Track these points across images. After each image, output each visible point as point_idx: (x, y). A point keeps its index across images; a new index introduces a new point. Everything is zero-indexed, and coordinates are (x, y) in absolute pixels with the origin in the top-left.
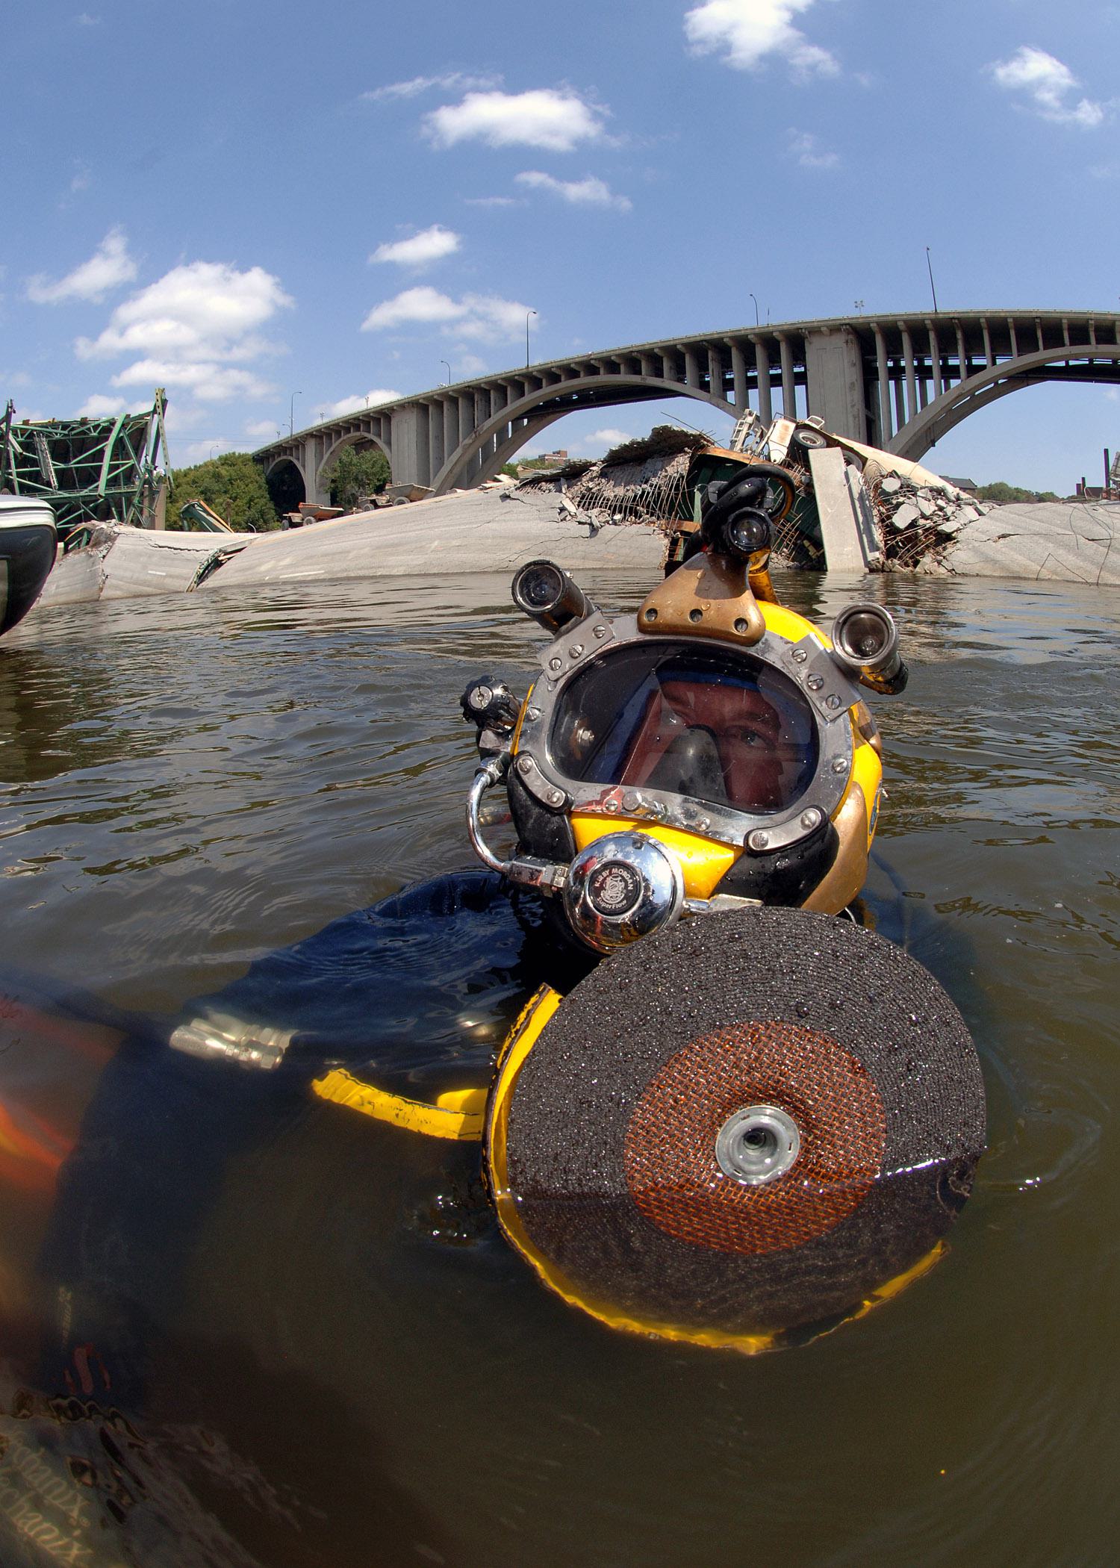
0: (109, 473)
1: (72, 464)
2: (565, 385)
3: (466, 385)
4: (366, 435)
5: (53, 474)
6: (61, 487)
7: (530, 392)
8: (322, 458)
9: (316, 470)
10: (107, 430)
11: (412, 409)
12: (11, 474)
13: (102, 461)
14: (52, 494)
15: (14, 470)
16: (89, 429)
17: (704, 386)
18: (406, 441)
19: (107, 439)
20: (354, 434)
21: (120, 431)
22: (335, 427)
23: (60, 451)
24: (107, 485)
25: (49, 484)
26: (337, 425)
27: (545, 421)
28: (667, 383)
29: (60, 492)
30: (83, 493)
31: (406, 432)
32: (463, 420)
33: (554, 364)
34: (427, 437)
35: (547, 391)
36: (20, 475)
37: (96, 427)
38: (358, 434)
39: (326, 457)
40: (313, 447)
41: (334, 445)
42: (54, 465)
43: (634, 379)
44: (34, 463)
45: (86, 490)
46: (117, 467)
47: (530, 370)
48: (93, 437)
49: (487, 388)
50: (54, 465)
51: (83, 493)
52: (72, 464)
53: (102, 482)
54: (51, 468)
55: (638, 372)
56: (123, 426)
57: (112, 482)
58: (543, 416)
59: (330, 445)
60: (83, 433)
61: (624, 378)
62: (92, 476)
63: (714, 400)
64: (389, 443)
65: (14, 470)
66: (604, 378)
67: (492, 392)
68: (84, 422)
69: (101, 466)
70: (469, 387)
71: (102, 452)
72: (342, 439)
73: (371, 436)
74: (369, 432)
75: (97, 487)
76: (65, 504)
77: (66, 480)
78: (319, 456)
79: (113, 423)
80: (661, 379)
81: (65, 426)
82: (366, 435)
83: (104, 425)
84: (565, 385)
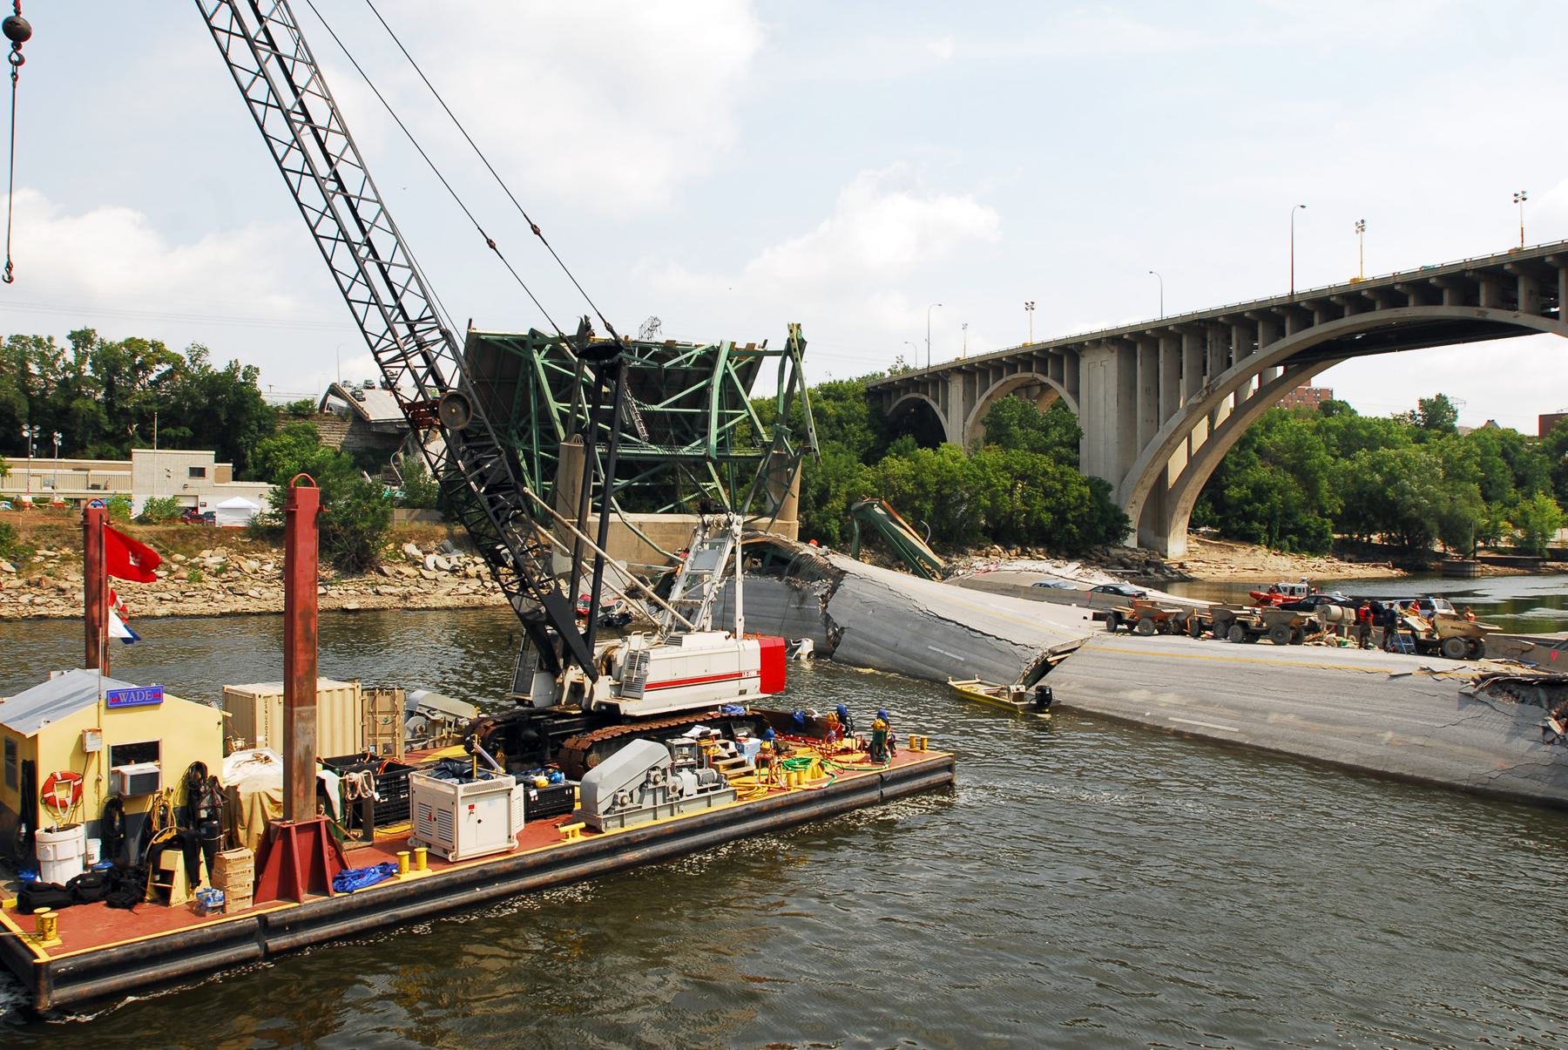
2: (1349, 321)
3: (1196, 317)
4: (1042, 378)
8: (973, 403)
9: (965, 420)
11: (1112, 348)
20: (1021, 375)
22: (995, 364)
26: (999, 360)
27: (1311, 370)
28: (1523, 319)
31: (1101, 375)
32: (1188, 368)
33: (1334, 292)
34: (1133, 387)
35: (1321, 330)
38: (1029, 375)
39: (979, 403)
40: (961, 387)
41: (992, 388)
47: (1296, 299)
58: (1313, 363)
61: (1447, 310)
64: (1075, 393)
66: (1414, 311)
67: (1234, 329)
70: (1200, 320)
72: (1003, 380)
73: (1048, 380)
74: (1046, 374)
78: (970, 400)
82: (1042, 378)
84: (1349, 321)
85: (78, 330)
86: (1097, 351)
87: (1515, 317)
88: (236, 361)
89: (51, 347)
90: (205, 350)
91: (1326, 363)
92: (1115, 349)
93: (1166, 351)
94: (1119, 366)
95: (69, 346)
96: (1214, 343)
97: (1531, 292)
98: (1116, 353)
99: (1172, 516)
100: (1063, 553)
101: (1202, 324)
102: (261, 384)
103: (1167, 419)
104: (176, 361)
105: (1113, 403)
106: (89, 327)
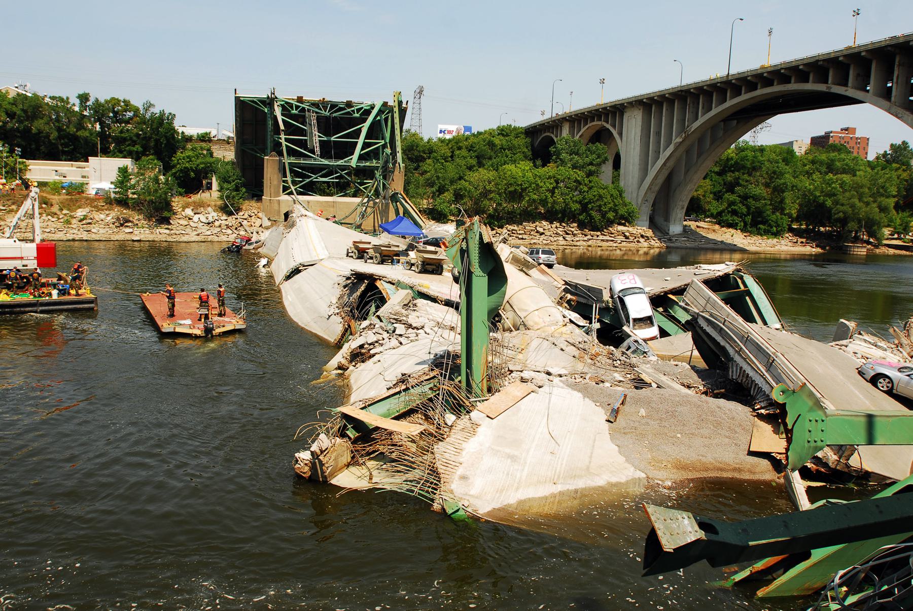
0: (362, 150)
1: (333, 139)
5: (318, 145)
6: (322, 156)
7: (732, 98)
10: (367, 112)
11: (640, 107)
12: (281, 139)
13: (358, 139)
14: (315, 159)
15: (283, 136)
16: (353, 111)
17: (886, 94)
18: (633, 132)
19: (364, 121)
21: (376, 116)
23: (326, 125)
24: (358, 160)
25: (313, 152)
28: (850, 92)
29: (322, 160)
30: (341, 162)
31: (633, 123)
32: (677, 120)
36: (286, 140)
37: (358, 110)
42: (319, 137)
43: (821, 87)
44: (302, 132)
45: (342, 161)
46: (369, 145)
48: (356, 118)
49: (711, 90)
50: (319, 137)
51: (341, 162)
52: (333, 139)
53: (355, 156)
54: (316, 138)
55: (826, 82)
56: (380, 112)
57: (361, 158)
59: (579, 130)
60: (348, 113)
61: (811, 86)
62: (346, 150)
63: (894, 109)
65: (283, 136)
68: (349, 104)
69: (365, 139)
71: (360, 130)
75: (351, 159)
76: (324, 169)
77: (327, 150)
79: (372, 107)
80: (844, 88)
81: (334, 106)
83: (366, 108)
85: (81, 93)
86: (632, 109)
87: (846, 91)
88: (163, 110)
89: (68, 103)
90: (154, 106)
91: (756, 120)
92: (641, 108)
93: (667, 110)
94: (642, 119)
95: (77, 102)
96: (691, 105)
97: (858, 75)
98: (641, 110)
99: (673, 209)
100: (588, 227)
101: (683, 93)
102: (177, 125)
103: (664, 151)
104: (137, 110)
105: (638, 142)
106: (86, 92)
